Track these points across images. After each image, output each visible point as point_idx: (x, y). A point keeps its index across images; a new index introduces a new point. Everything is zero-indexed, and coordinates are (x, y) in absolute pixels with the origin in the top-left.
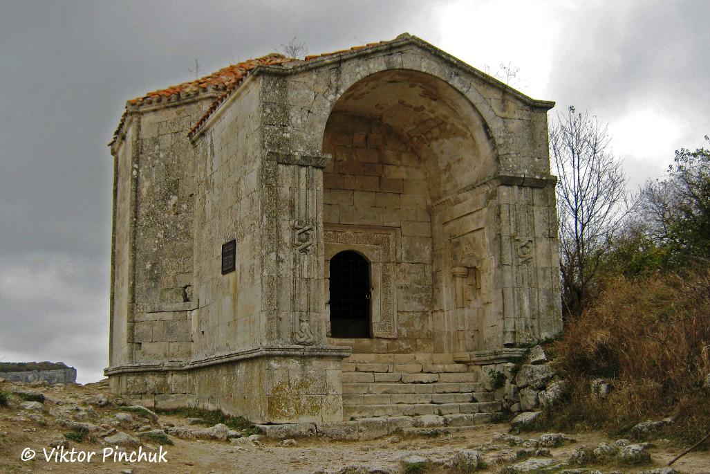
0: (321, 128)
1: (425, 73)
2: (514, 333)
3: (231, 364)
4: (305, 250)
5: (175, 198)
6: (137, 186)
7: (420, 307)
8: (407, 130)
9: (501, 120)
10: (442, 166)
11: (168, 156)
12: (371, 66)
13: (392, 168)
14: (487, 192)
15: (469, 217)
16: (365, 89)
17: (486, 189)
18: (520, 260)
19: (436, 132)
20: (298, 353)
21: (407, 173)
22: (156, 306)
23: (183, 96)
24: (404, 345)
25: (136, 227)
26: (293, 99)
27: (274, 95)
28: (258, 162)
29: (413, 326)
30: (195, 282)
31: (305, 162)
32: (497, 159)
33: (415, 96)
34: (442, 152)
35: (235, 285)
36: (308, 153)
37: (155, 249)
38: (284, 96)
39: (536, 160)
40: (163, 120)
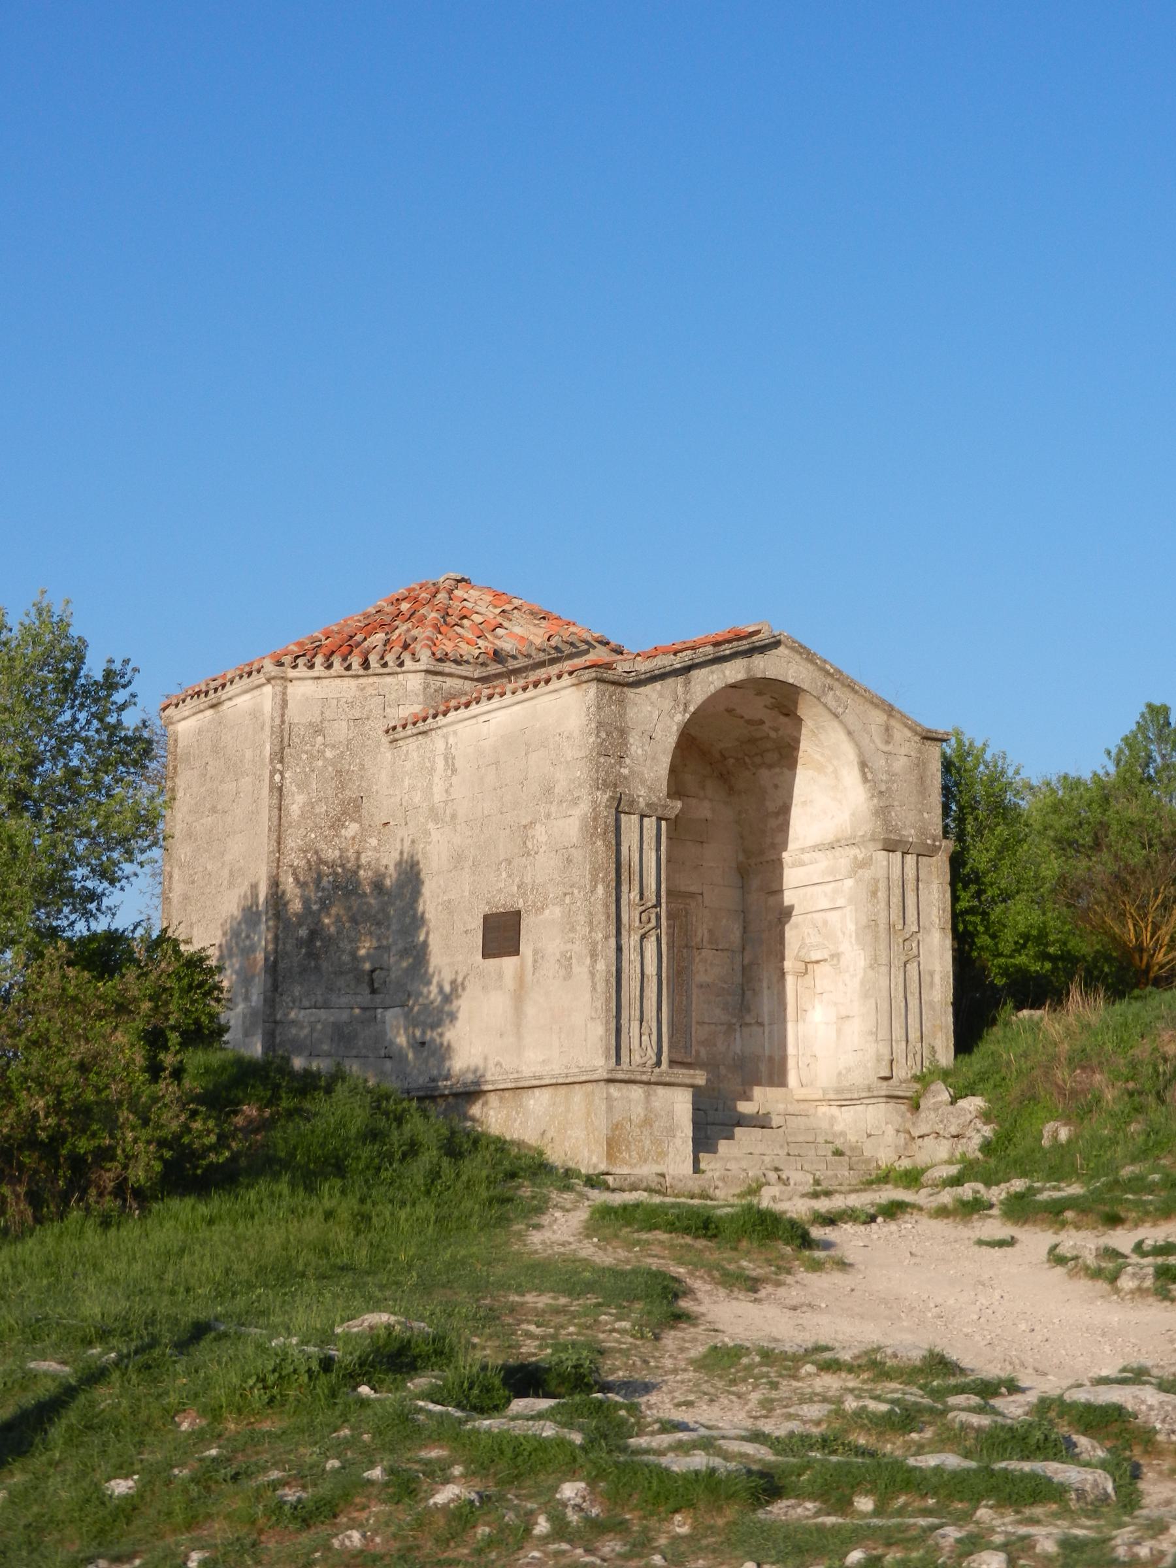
0: (665, 761)
1: (792, 685)
6: (281, 800)
9: (883, 755)
10: (771, 806)
11: (341, 756)
12: (727, 673)
14: (855, 857)
20: (645, 1078)
25: (278, 867)
26: (632, 718)
28: (584, 808)
29: (715, 1045)
33: (757, 708)
34: (776, 786)
36: (654, 799)
38: (622, 715)
39: (926, 815)
40: (331, 695)
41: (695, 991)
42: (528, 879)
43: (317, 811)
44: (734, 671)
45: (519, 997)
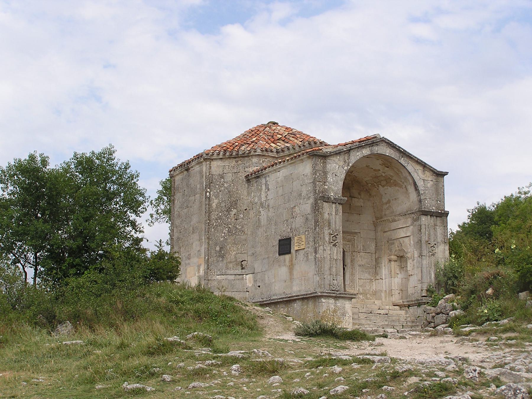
0: (341, 183)
3: (288, 301)
4: (335, 245)
5: (234, 211)
7: (369, 277)
10: (384, 201)
12: (364, 152)
13: (356, 200)
19: (384, 183)
20: (334, 295)
23: (240, 153)
27: (320, 166)
28: (311, 200)
30: (250, 259)
32: (420, 201)
33: (377, 164)
35: (291, 260)
36: (337, 197)
37: (222, 239)
38: (324, 167)
41: (357, 268)
42: (293, 227)
43: (222, 205)
44: (366, 152)
45: (291, 268)
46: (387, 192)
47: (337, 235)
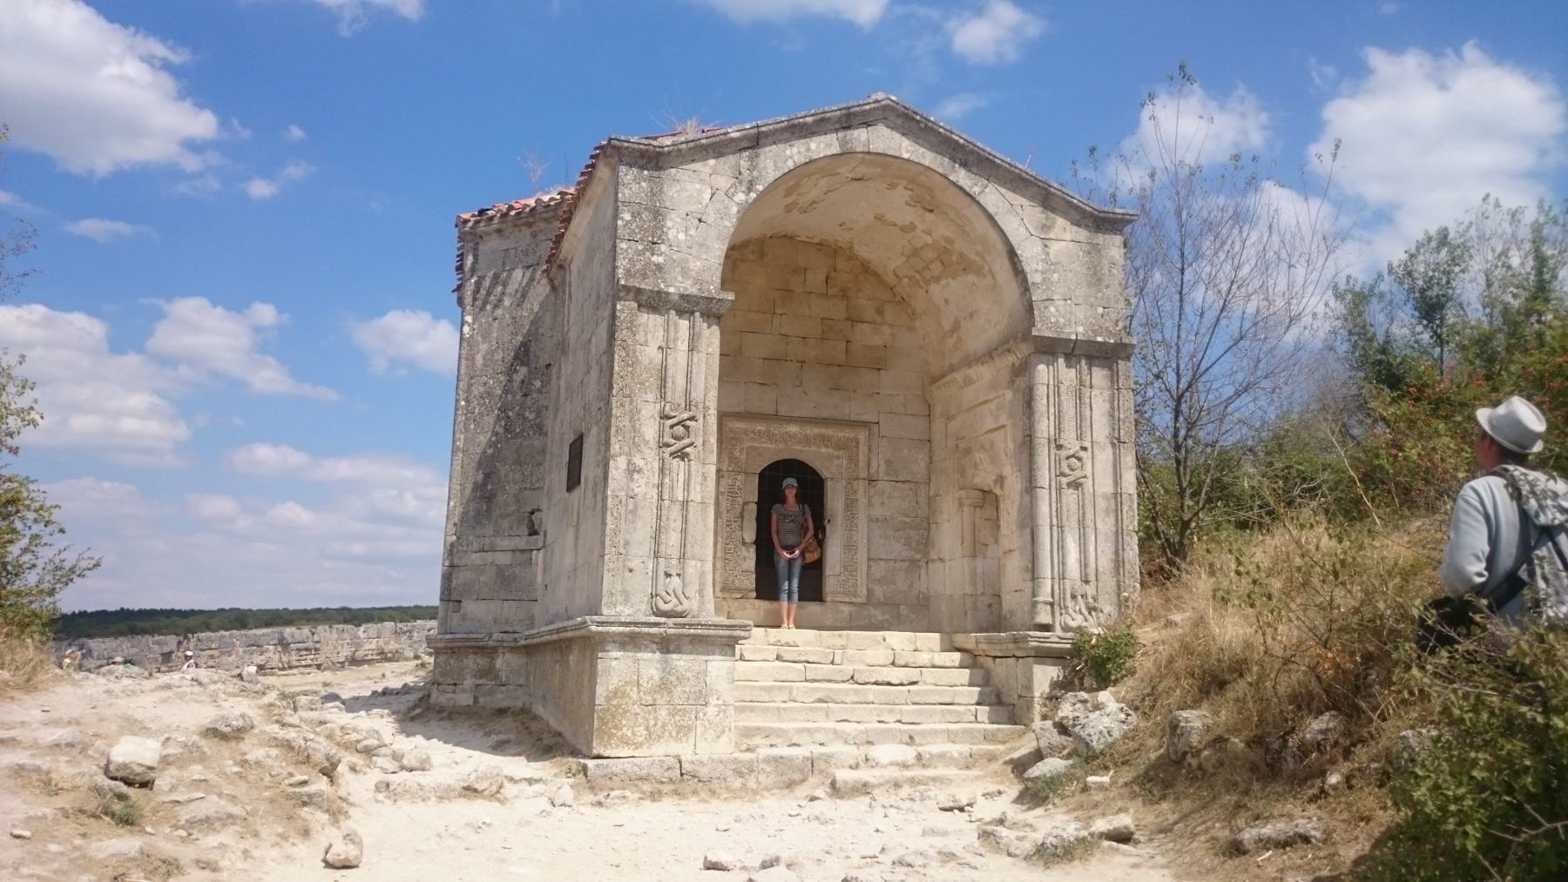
1: (908, 160)
2: (1052, 604)
4: (682, 455)
7: (907, 554)
8: (892, 265)
9: (1039, 242)
12: (813, 146)
15: (986, 406)
16: (815, 193)
17: (1011, 359)
18: (1064, 480)
19: (936, 268)
20: (654, 630)
21: (893, 336)
22: (487, 541)
24: (878, 614)
30: (544, 506)
31: (687, 306)
34: (946, 301)
36: (693, 290)
38: (653, 194)
44: (822, 146)
46: (949, 292)
47: (692, 418)
